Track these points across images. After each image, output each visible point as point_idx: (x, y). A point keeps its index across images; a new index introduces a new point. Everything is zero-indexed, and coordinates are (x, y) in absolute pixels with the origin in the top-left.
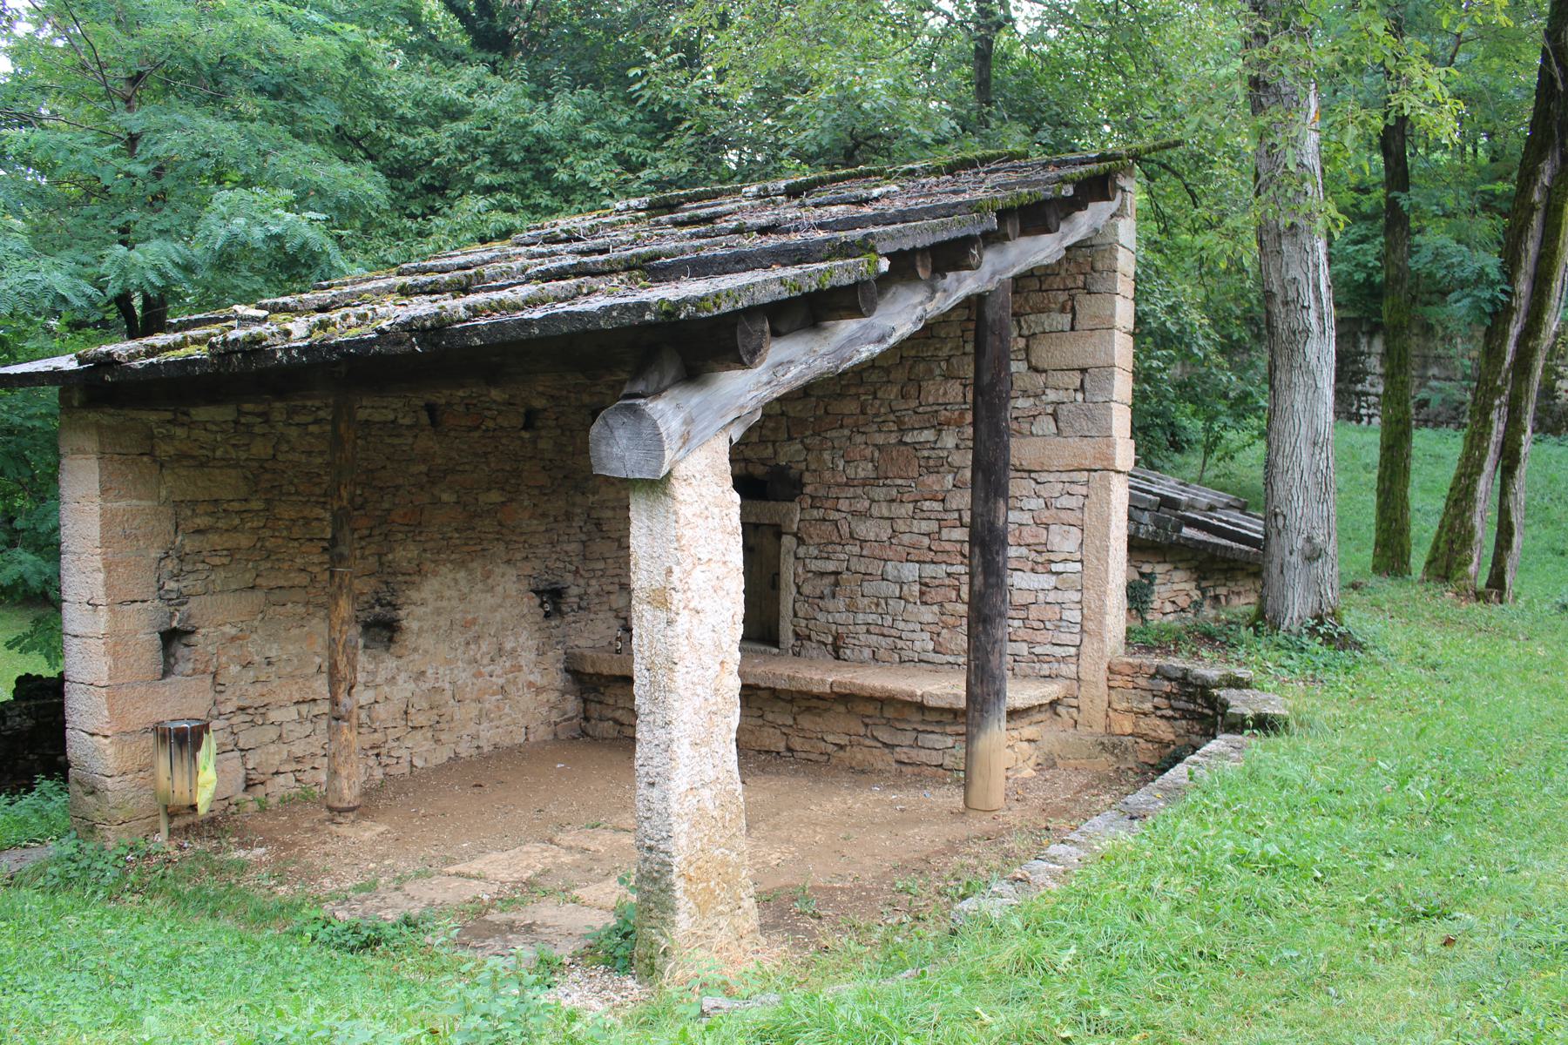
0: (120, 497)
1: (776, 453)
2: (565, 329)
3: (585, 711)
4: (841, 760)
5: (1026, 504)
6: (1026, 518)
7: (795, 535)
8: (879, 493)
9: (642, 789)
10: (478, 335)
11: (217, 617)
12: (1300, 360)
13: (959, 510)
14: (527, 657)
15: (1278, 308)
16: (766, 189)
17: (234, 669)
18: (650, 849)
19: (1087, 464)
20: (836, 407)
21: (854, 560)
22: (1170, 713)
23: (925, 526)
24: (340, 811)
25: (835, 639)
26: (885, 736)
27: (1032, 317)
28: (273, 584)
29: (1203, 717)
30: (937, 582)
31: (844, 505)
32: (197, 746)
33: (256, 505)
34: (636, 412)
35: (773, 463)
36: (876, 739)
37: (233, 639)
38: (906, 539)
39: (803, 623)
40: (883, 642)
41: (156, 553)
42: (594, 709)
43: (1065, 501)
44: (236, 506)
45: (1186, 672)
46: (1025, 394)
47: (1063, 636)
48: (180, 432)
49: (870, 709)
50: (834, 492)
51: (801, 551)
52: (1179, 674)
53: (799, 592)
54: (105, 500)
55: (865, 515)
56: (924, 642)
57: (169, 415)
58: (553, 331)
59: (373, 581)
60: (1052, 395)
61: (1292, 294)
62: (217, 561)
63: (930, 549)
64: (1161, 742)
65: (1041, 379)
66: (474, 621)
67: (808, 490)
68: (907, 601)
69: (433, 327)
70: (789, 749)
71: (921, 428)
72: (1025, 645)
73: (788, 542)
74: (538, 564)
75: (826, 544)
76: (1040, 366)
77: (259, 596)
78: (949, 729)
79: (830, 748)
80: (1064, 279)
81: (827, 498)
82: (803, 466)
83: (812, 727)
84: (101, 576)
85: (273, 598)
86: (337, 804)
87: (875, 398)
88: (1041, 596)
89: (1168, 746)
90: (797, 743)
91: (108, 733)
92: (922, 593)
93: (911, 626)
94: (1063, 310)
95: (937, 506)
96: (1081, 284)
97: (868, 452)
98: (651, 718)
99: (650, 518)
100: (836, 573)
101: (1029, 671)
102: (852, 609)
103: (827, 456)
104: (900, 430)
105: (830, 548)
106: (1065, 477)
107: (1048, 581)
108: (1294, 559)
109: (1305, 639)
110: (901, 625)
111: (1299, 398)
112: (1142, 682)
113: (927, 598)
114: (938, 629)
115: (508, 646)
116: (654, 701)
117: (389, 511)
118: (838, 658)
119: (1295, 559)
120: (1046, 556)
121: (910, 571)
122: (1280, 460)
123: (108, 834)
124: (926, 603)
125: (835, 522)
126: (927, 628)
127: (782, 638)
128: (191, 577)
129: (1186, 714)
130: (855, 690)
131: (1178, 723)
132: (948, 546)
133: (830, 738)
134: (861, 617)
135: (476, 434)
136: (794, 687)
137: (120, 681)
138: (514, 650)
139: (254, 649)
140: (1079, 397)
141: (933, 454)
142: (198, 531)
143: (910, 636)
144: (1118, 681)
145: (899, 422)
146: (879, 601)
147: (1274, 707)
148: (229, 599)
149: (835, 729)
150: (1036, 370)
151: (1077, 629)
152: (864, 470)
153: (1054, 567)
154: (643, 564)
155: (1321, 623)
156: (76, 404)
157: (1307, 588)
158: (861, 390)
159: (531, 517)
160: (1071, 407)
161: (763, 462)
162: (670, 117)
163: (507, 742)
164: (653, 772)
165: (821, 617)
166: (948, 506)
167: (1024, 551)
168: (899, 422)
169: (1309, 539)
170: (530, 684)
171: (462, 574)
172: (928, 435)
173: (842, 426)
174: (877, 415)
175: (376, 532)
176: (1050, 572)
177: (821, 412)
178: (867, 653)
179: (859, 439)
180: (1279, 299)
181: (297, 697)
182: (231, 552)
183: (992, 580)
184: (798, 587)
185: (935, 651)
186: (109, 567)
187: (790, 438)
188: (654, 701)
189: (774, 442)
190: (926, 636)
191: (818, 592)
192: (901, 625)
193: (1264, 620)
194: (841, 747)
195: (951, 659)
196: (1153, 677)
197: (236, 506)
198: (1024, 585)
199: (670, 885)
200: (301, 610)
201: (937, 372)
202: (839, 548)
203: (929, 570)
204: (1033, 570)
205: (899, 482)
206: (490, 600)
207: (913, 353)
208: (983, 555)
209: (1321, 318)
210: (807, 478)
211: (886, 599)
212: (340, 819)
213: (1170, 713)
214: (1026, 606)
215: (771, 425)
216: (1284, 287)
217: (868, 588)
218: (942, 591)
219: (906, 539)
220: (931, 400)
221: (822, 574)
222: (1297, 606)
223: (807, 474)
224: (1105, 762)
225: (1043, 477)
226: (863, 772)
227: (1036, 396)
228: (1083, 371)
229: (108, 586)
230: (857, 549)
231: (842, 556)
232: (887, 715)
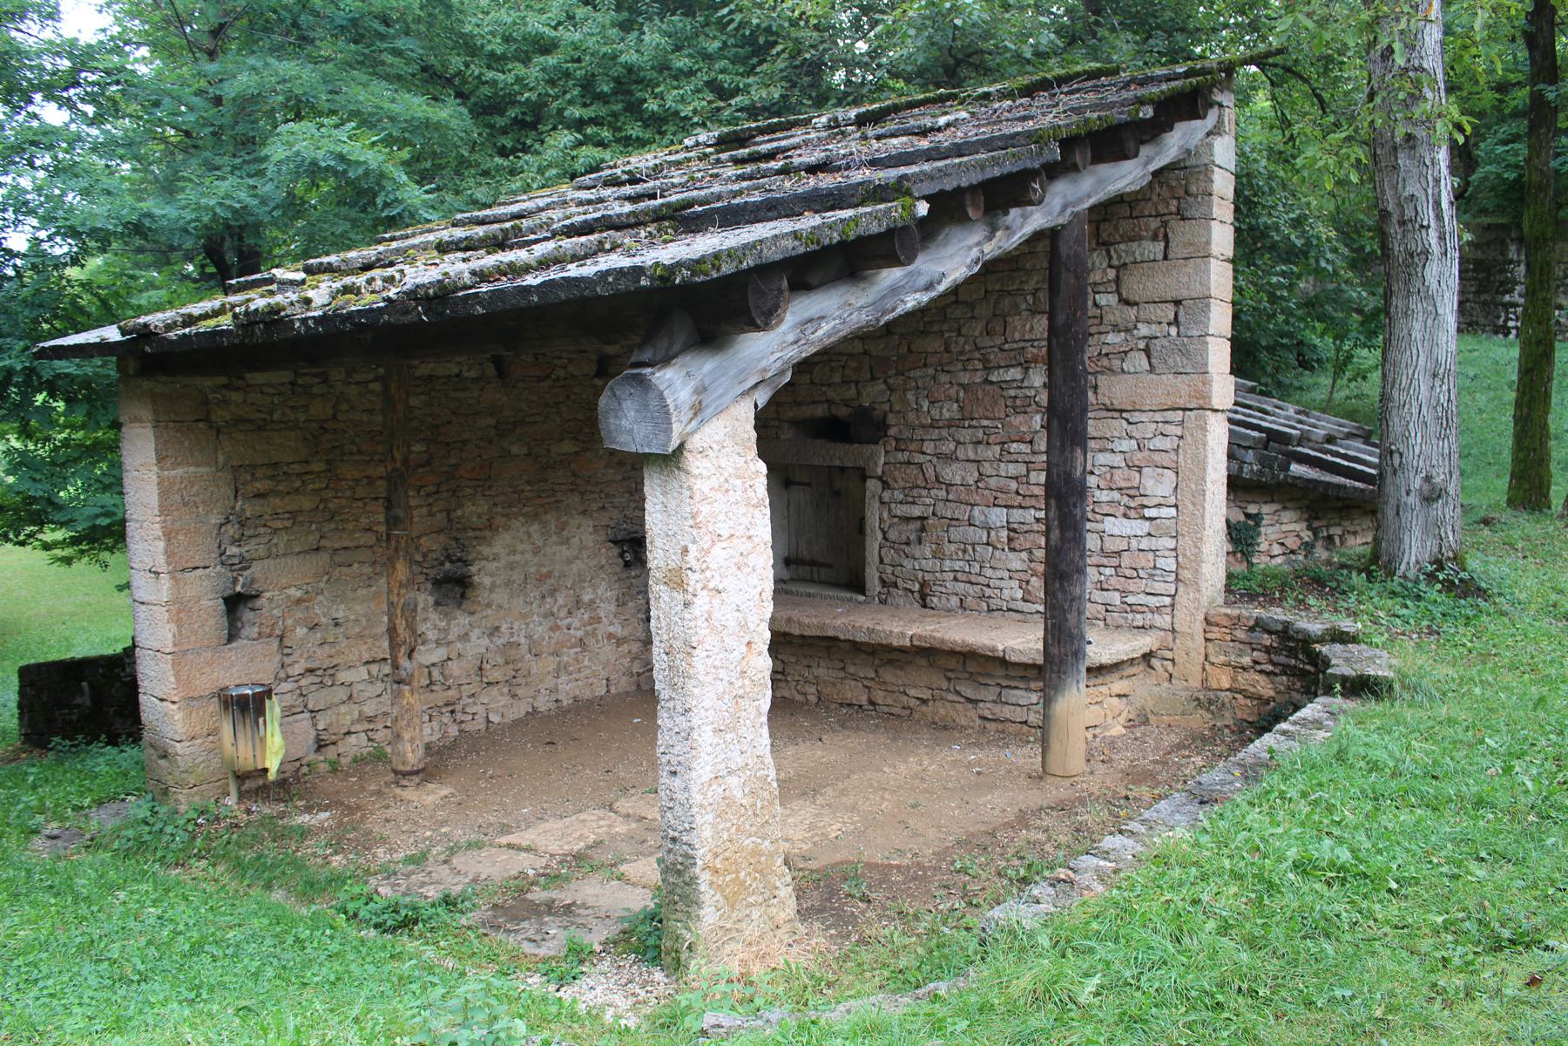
0: (176, 465)
1: (859, 393)
2: (563, 296)
4: (924, 715)
5: (1117, 446)
6: (1117, 460)
7: (880, 478)
8: (965, 435)
9: (665, 779)
10: (480, 303)
11: (282, 582)
12: (1418, 284)
14: (606, 609)
15: (1394, 229)
16: (836, 119)
17: (301, 631)
18: (674, 840)
19: (1181, 403)
22: (1270, 668)
23: (1013, 469)
24: (405, 774)
25: (923, 585)
26: (969, 692)
27: (1123, 247)
28: (337, 545)
29: (1303, 674)
30: (1025, 528)
31: (929, 447)
32: (260, 711)
33: (317, 466)
34: (643, 383)
35: (855, 404)
36: (958, 693)
37: (299, 601)
38: (993, 482)
39: (889, 570)
40: (971, 589)
41: (215, 519)
43: (1159, 443)
44: (297, 468)
45: (1287, 625)
46: (1116, 328)
47: (1157, 585)
48: (236, 397)
49: (952, 663)
50: (919, 433)
51: (887, 496)
52: (1280, 627)
53: (885, 538)
54: (161, 469)
55: (950, 458)
57: (223, 380)
59: (442, 538)
61: (1409, 213)
62: (279, 524)
63: (1017, 493)
64: (1260, 698)
65: (1132, 313)
66: (549, 575)
67: (892, 432)
68: (995, 548)
69: (436, 296)
70: (871, 703)
71: (1008, 366)
72: (1117, 594)
73: (873, 485)
74: (615, 514)
75: (912, 488)
76: (1131, 298)
77: (324, 557)
78: (1033, 685)
79: (913, 703)
80: (1155, 205)
82: (887, 407)
83: (894, 680)
84: (161, 544)
85: (338, 559)
86: (401, 768)
87: (959, 334)
88: (1134, 542)
89: (1267, 702)
90: (879, 696)
91: (176, 699)
92: (1010, 540)
93: (999, 574)
94: (1155, 238)
95: (1024, 448)
96: (1173, 209)
99: (665, 493)
101: (1122, 622)
102: (938, 555)
103: (910, 396)
104: (985, 368)
106: (1158, 416)
107: (1142, 527)
108: (1411, 500)
109: (1422, 586)
110: (989, 573)
111: (1417, 326)
112: (1241, 635)
113: (1016, 545)
114: (1024, 577)
115: (586, 598)
116: (673, 686)
117: (457, 466)
118: (925, 606)
120: (1139, 500)
121: (998, 516)
122: (1396, 395)
123: (180, 797)
124: (1013, 550)
125: (920, 465)
126: (1015, 575)
128: (254, 541)
129: (1286, 670)
131: (1278, 679)
133: (912, 692)
135: (546, 384)
136: (874, 640)
137: (185, 647)
138: (592, 601)
139: (320, 610)
140: (1173, 331)
142: (259, 495)
143: (998, 583)
144: (1215, 633)
145: (985, 360)
146: (966, 547)
147: (1379, 666)
148: (293, 562)
149: (918, 684)
150: (1127, 303)
151: (1172, 577)
152: (949, 411)
153: (1147, 513)
154: (659, 542)
155: (1441, 568)
156: (131, 372)
157: (1425, 531)
158: (945, 327)
159: (607, 466)
160: (1165, 342)
161: (846, 403)
162: (761, 40)
163: (587, 694)
164: (674, 760)
165: (908, 564)
167: (1116, 495)
168: (985, 360)
169: (1428, 479)
170: (610, 636)
171: (535, 527)
172: (1014, 373)
173: (925, 365)
174: (961, 353)
175: (444, 488)
176: (1144, 517)
178: (954, 601)
179: (944, 378)
180: (1395, 219)
181: (366, 657)
182: (293, 515)
183: (1070, 535)
186: (168, 535)
187: (873, 379)
188: (673, 686)
189: (857, 383)
190: (1015, 584)
191: (904, 538)
192: (989, 573)
193: (1379, 564)
194: (924, 701)
196: (1252, 629)
197: (297, 468)
198: (1116, 531)
199: (694, 879)
200: (367, 569)
201: (1024, 306)
202: (924, 493)
203: (1017, 515)
204: (1125, 516)
205: (986, 423)
206: (565, 552)
207: (998, 287)
208: (1059, 508)
209: (1442, 238)
210: (891, 419)
211: (973, 545)
212: (405, 782)
213: (1270, 668)
214: (1119, 553)
215: (854, 364)
216: (1400, 205)
217: (955, 534)
218: (1031, 537)
219: (993, 482)
220: (1017, 336)
221: (908, 519)
222: (1415, 550)
223: (891, 416)
224: (1200, 720)
225: (1136, 417)
226: (945, 728)
227: (1127, 330)
228: (1177, 303)
229: (169, 554)
230: (943, 493)
231: (928, 501)
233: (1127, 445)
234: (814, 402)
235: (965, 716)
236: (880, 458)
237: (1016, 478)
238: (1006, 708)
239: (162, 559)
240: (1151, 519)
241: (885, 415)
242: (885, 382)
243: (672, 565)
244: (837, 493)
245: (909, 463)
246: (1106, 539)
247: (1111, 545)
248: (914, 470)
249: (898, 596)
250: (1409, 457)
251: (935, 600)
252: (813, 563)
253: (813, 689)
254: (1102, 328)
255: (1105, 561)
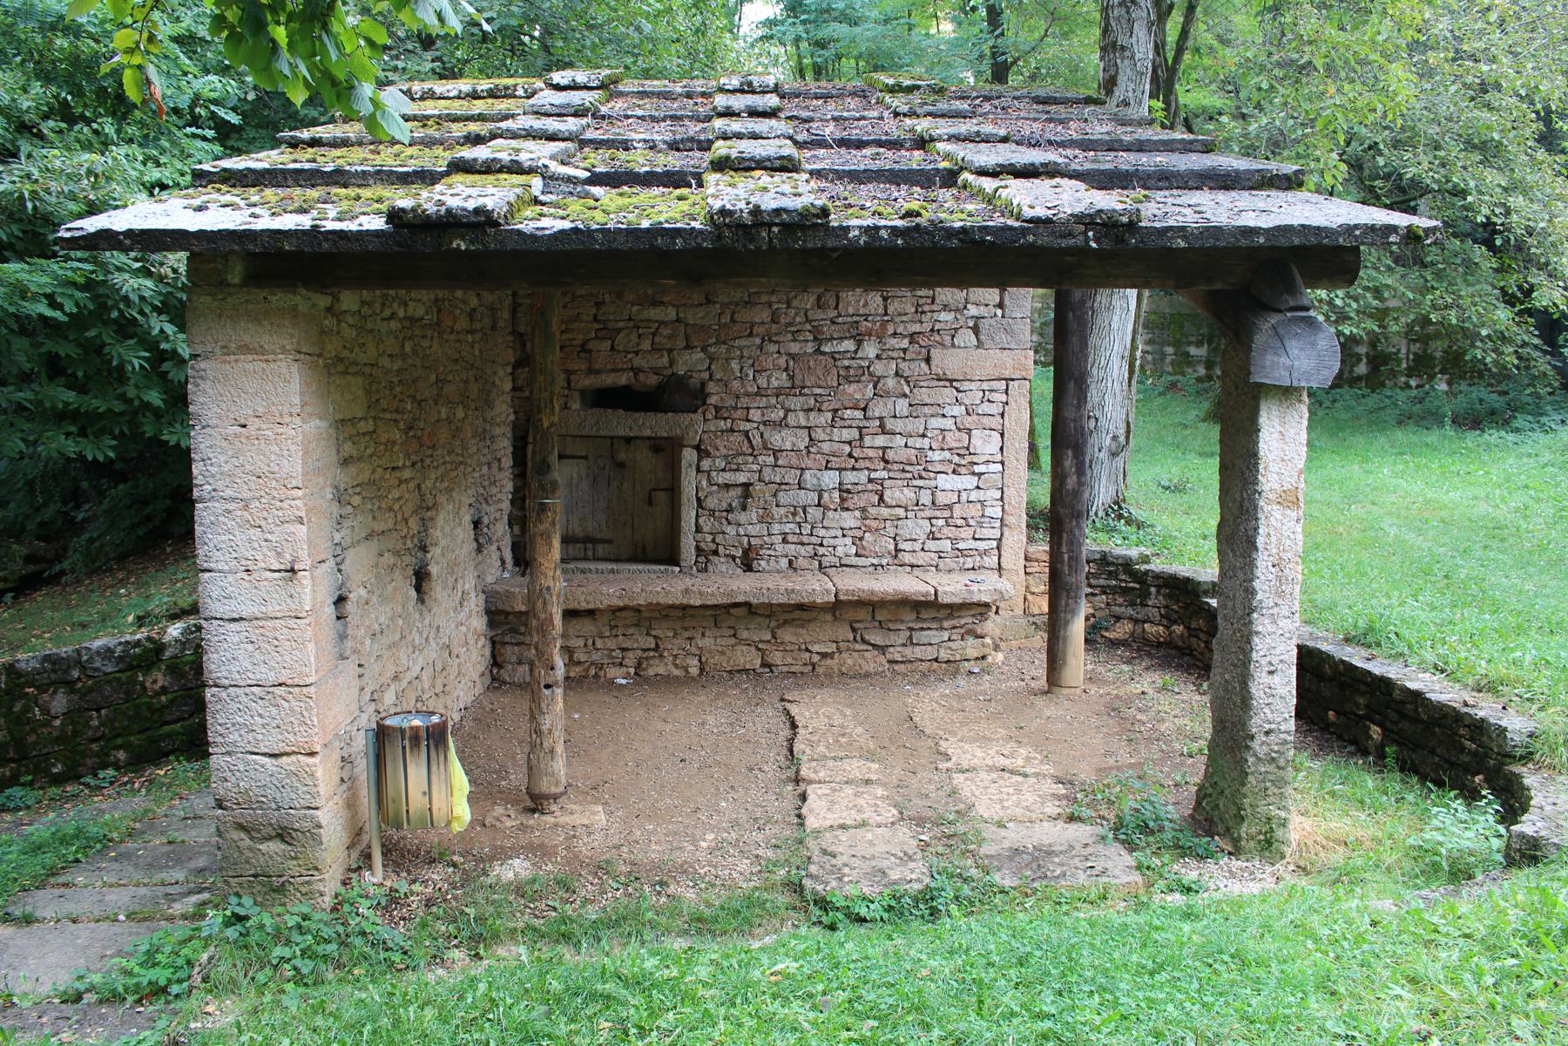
3: (493, 655)
5: (948, 411)
6: (948, 423)
7: (698, 448)
8: (795, 402)
10: (1184, 238)
13: (881, 419)
18: (1267, 733)
19: (1007, 374)
20: (744, 315)
21: (767, 472)
23: (847, 434)
25: (746, 552)
26: (879, 640)
29: (1125, 591)
30: (860, 488)
31: (755, 415)
35: (669, 372)
40: (802, 550)
42: (510, 653)
43: (986, 408)
46: (946, 308)
49: (863, 614)
50: (744, 401)
51: (706, 464)
52: (1097, 556)
55: (782, 424)
56: (845, 547)
58: (1283, 242)
60: (973, 310)
63: (850, 455)
67: (713, 400)
71: (841, 339)
73: (689, 455)
75: (735, 456)
78: (946, 624)
79: (816, 658)
81: (736, 408)
82: (706, 375)
83: (794, 639)
87: (789, 307)
88: (964, 496)
90: (776, 657)
91: (317, 748)
92: (843, 500)
93: (832, 533)
95: (859, 414)
97: (782, 361)
98: (1275, 611)
100: (746, 486)
103: (735, 365)
104: (816, 339)
105: (740, 459)
106: (985, 386)
110: (822, 532)
111: (1116, 318)
114: (858, 533)
119: (1103, 455)
120: (969, 458)
121: (830, 479)
122: (1095, 371)
125: (746, 434)
126: (850, 533)
127: (683, 556)
130: (864, 596)
132: (871, 453)
134: (776, 528)
136: (794, 599)
140: (999, 312)
141: (854, 363)
143: (832, 541)
149: (821, 638)
151: (998, 524)
152: (779, 380)
153: (977, 469)
154: (1274, 467)
156: (235, 278)
157: (1109, 480)
158: (774, 299)
160: (992, 321)
164: (1275, 660)
166: (869, 413)
167: (947, 455)
169: (1115, 438)
172: (848, 345)
173: (751, 335)
174: (790, 324)
176: (973, 473)
177: (726, 319)
178: (784, 562)
179: (773, 348)
184: (698, 499)
185: (857, 555)
187: (688, 347)
189: (670, 351)
190: (848, 541)
191: (725, 505)
192: (822, 532)
194: (824, 655)
195: (875, 561)
198: (948, 487)
202: (751, 459)
203: (850, 477)
204: (954, 472)
205: (818, 391)
208: (1076, 456)
210: (712, 387)
212: (554, 808)
214: (950, 507)
217: (783, 497)
219: (826, 447)
220: (851, 311)
221: (727, 486)
225: (965, 386)
227: (957, 310)
230: (772, 458)
231: (755, 467)
232: (878, 618)
233: (958, 410)
234: (613, 370)
235: (872, 662)
236: (696, 426)
237: (850, 443)
238: (918, 648)
239: (304, 554)
240: (980, 475)
241: (703, 384)
242: (704, 350)
243: (1287, 486)
244: (621, 465)
245: (732, 430)
246: (938, 493)
247: (942, 499)
248: (739, 438)
249: (721, 564)
250: (1103, 422)
251: (763, 563)
252: (588, 540)
253: (696, 662)
254: (935, 307)
255: (938, 513)
